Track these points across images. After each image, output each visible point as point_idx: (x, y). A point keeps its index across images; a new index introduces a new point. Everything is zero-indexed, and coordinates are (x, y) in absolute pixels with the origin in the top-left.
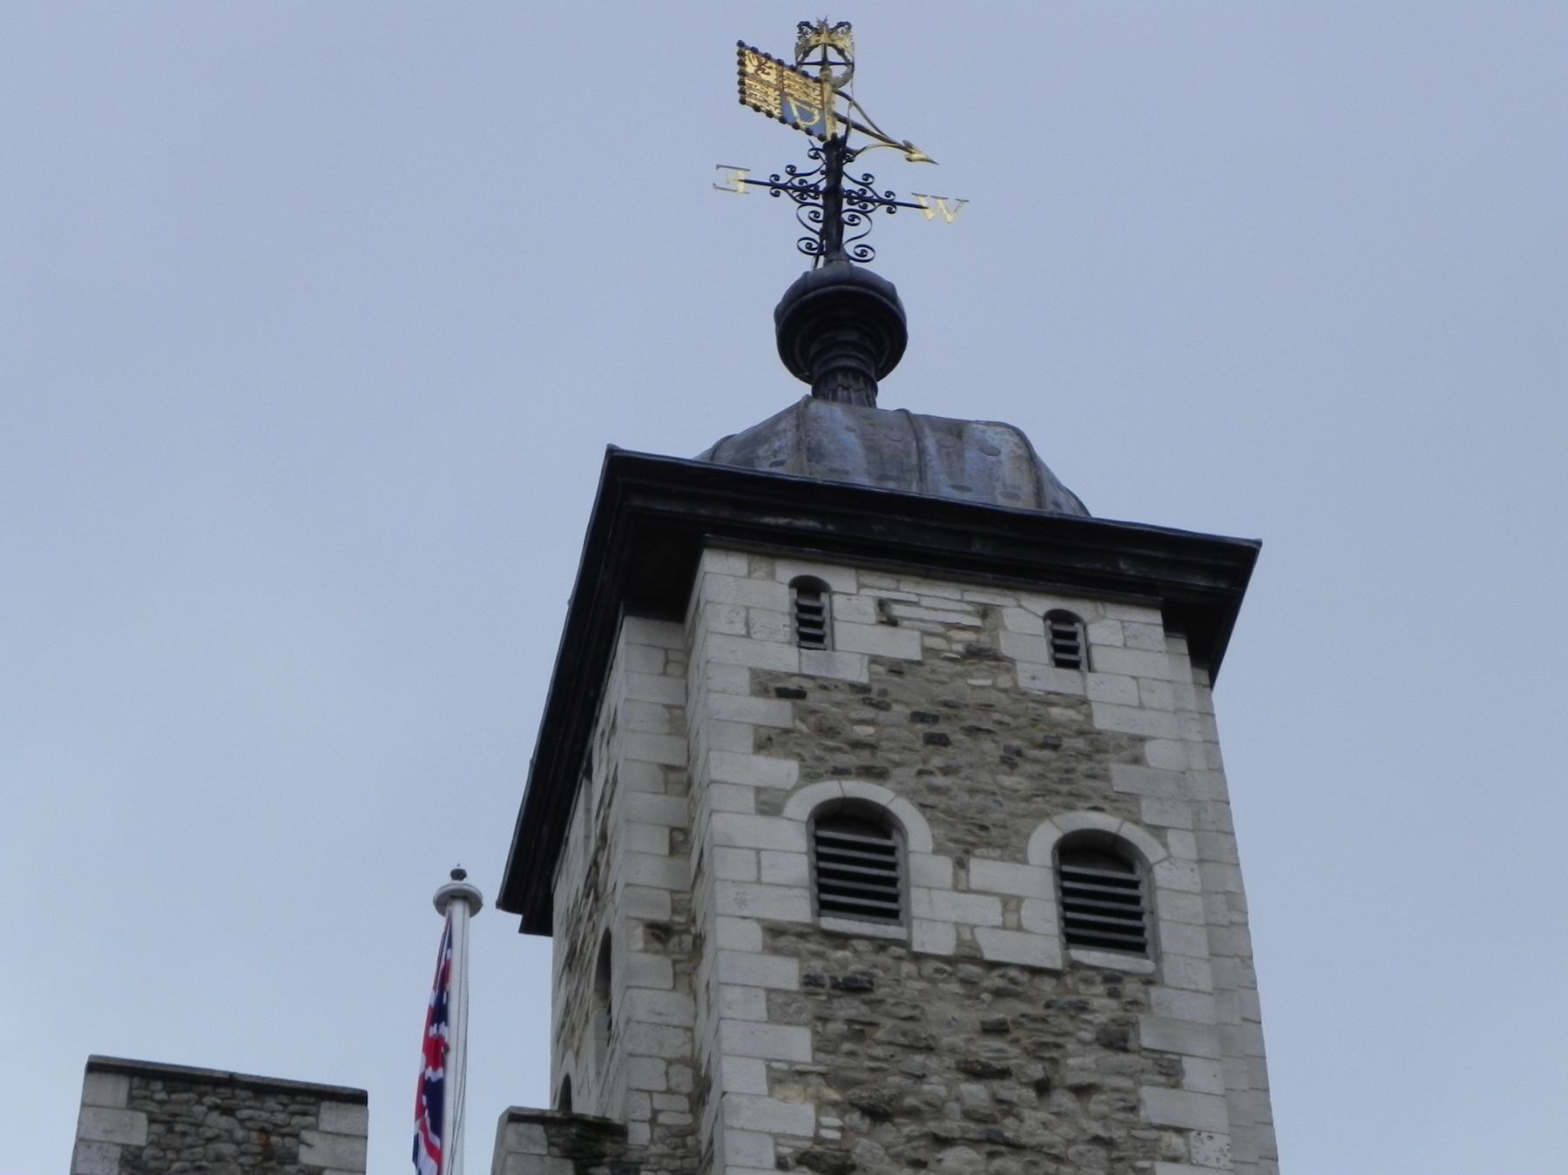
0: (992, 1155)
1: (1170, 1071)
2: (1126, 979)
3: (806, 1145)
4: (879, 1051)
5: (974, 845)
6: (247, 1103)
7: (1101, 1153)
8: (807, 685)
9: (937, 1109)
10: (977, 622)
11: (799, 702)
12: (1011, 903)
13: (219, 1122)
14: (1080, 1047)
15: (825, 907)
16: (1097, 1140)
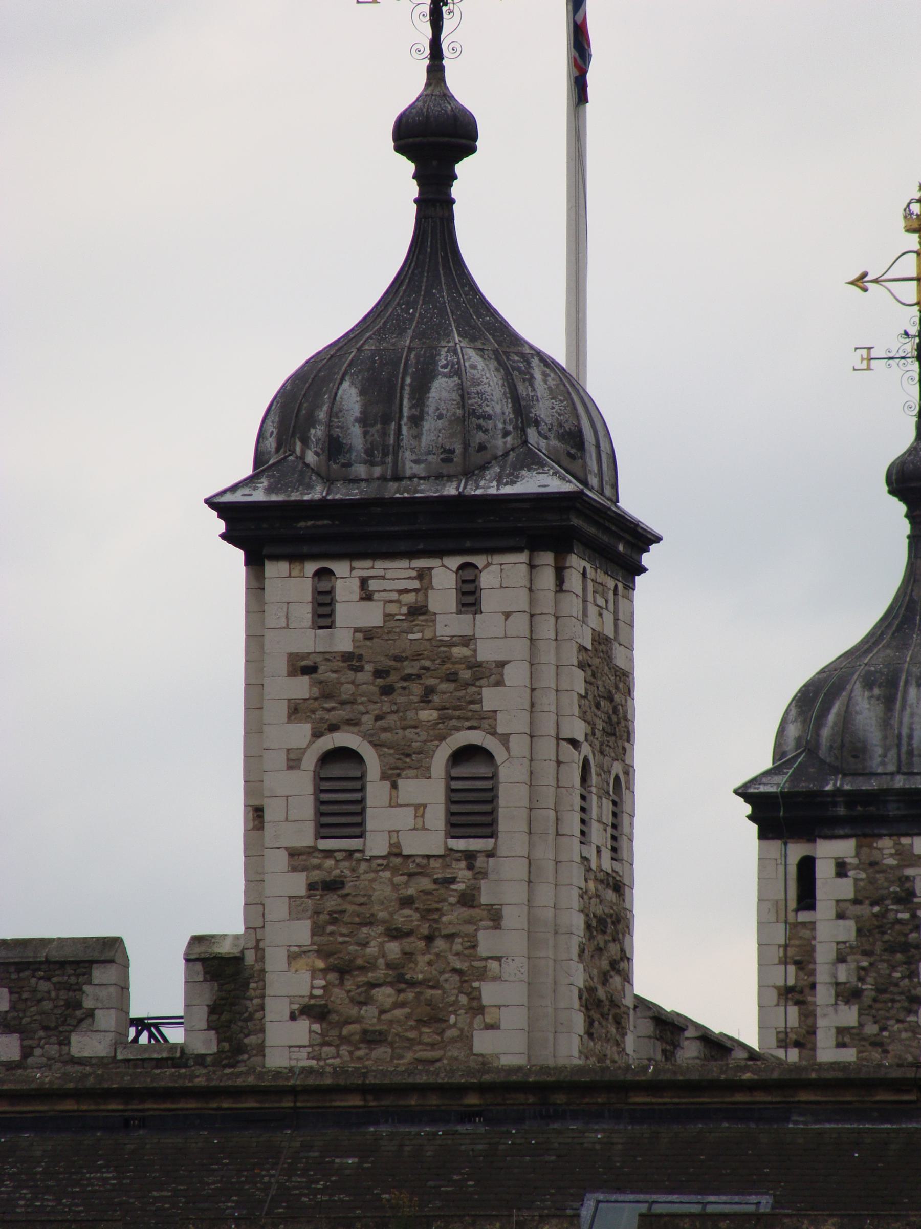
0: (400, 991)
1: (495, 917)
2: (479, 855)
3: (306, 1000)
4: (344, 931)
5: (403, 769)
6: (57, 973)
7: (457, 978)
8: (319, 659)
9: (370, 966)
10: (416, 584)
11: (314, 676)
12: (420, 809)
13: (44, 986)
14: (449, 908)
15: (319, 836)
16: (455, 971)
